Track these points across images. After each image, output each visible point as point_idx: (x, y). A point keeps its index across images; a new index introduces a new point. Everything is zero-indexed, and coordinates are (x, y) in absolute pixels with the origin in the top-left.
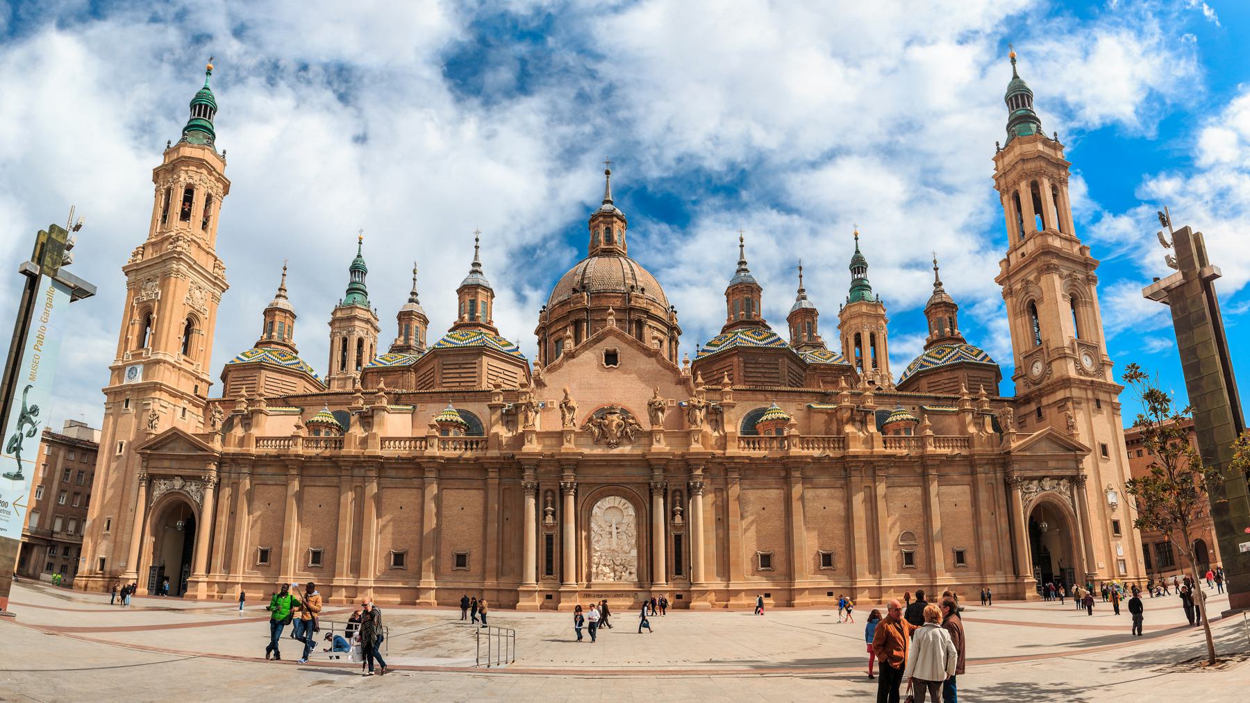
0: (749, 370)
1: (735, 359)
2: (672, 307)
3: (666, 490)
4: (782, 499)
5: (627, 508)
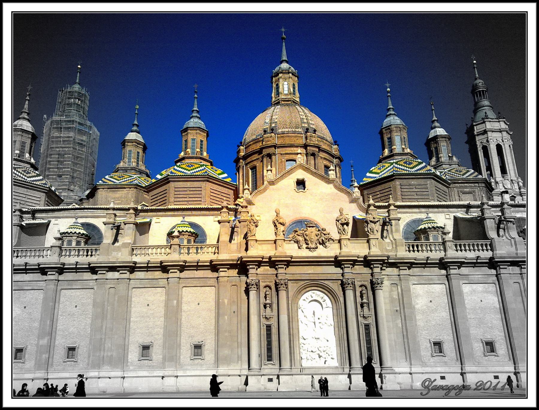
0: (405, 190)
3: (353, 284)
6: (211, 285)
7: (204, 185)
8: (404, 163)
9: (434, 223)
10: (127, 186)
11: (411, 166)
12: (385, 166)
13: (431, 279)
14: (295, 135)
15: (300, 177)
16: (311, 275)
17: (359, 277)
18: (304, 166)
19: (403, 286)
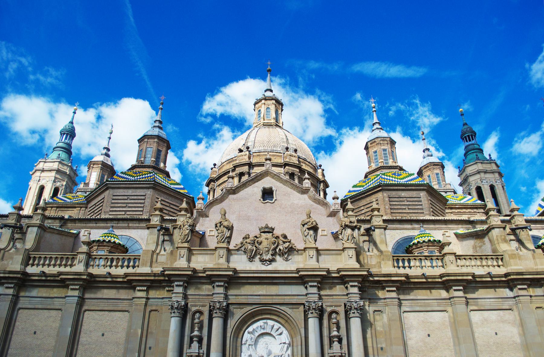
0: (394, 203)
1: (380, 195)
2: (320, 166)
4: (447, 323)
5: (281, 334)
6: (124, 309)
7: (149, 193)
9: (430, 237)
10: (78, 205)
11: (401, 177)
12: (370, 179)
13: (429, 305)
14: (273, 153)
15: (267, 186)
16: (261, 297)
17: (329, 300)
18: (273, 173)
19: (390, 313)
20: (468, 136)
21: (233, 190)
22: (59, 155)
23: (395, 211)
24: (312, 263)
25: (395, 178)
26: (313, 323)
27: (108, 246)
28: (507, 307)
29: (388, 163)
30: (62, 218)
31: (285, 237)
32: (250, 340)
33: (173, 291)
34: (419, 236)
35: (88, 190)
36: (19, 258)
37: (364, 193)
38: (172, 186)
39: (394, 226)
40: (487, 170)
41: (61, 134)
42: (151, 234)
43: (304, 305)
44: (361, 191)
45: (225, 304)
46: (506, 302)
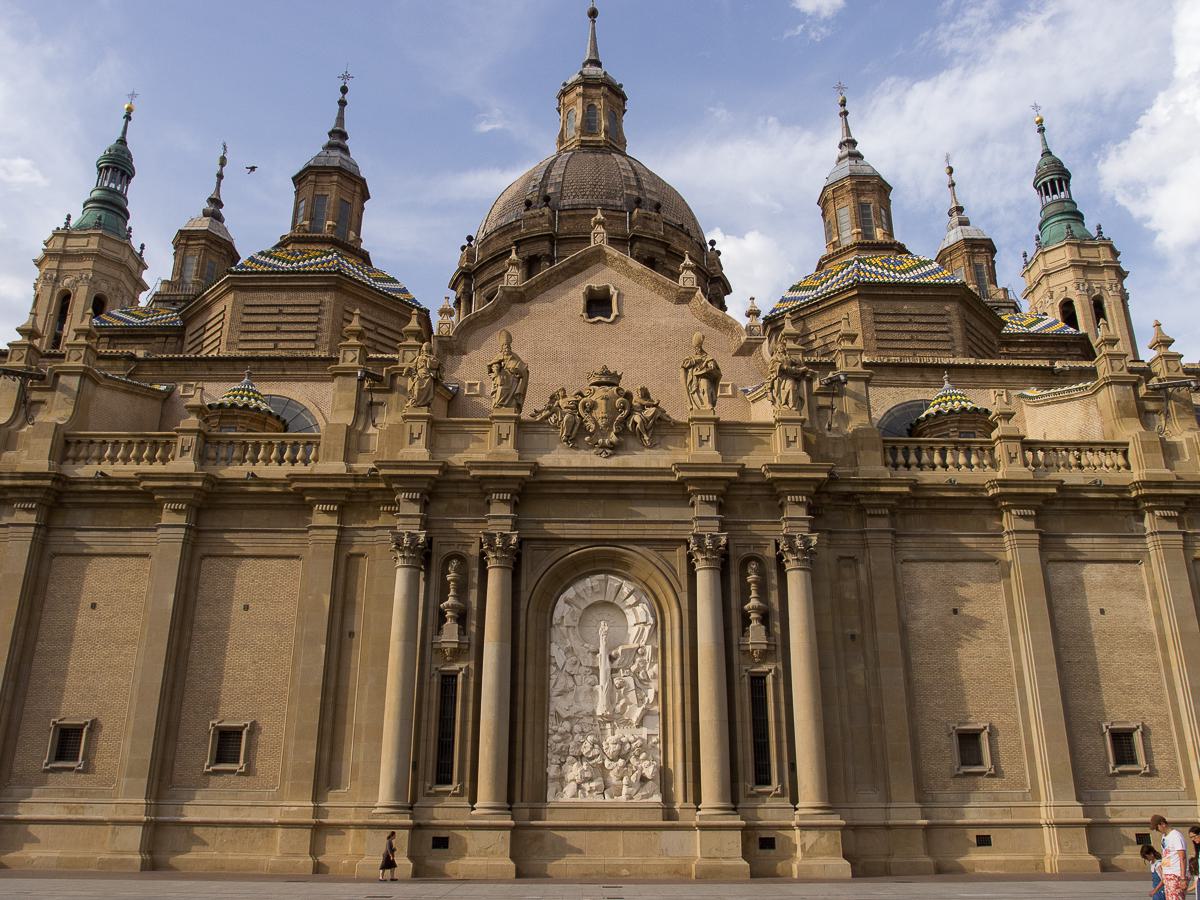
0: (885, 327)
1: (854, 308)
6: (288, 552)
8: (882, 261)
10: (159, 331)
20: (1052, 181)
21: (520, 292)
22: (100, 218)
23: (885, 345)
24: (706, 453)
25: (889, 270)
26: (704, 579)
27: (244, 418)
28: (1131, 557)
29: (871, 237)
30: (132, 358)
31: (645, 394)
32: (568, 616)
33: (398, 511)
34: (939, 400)
35: (178, 298)
36: (45, 445)
37: (817, 304)
38: (379, 285)
39: (883, 378)
40: (1089, 262)
41: (100, 170)
42: (341, 388)
43: (688, 544)
44: (811, 298)
45: (514, 539)
46: (1128, 546)
